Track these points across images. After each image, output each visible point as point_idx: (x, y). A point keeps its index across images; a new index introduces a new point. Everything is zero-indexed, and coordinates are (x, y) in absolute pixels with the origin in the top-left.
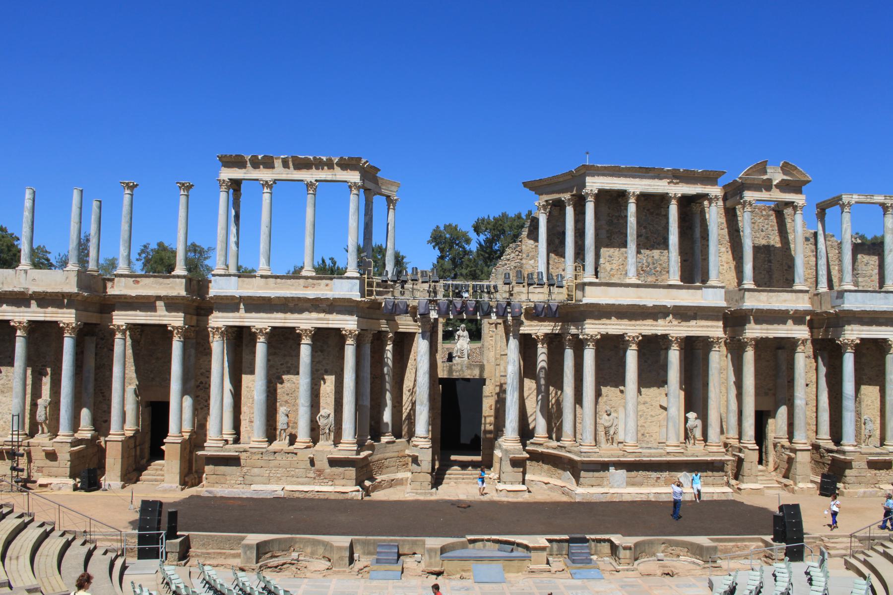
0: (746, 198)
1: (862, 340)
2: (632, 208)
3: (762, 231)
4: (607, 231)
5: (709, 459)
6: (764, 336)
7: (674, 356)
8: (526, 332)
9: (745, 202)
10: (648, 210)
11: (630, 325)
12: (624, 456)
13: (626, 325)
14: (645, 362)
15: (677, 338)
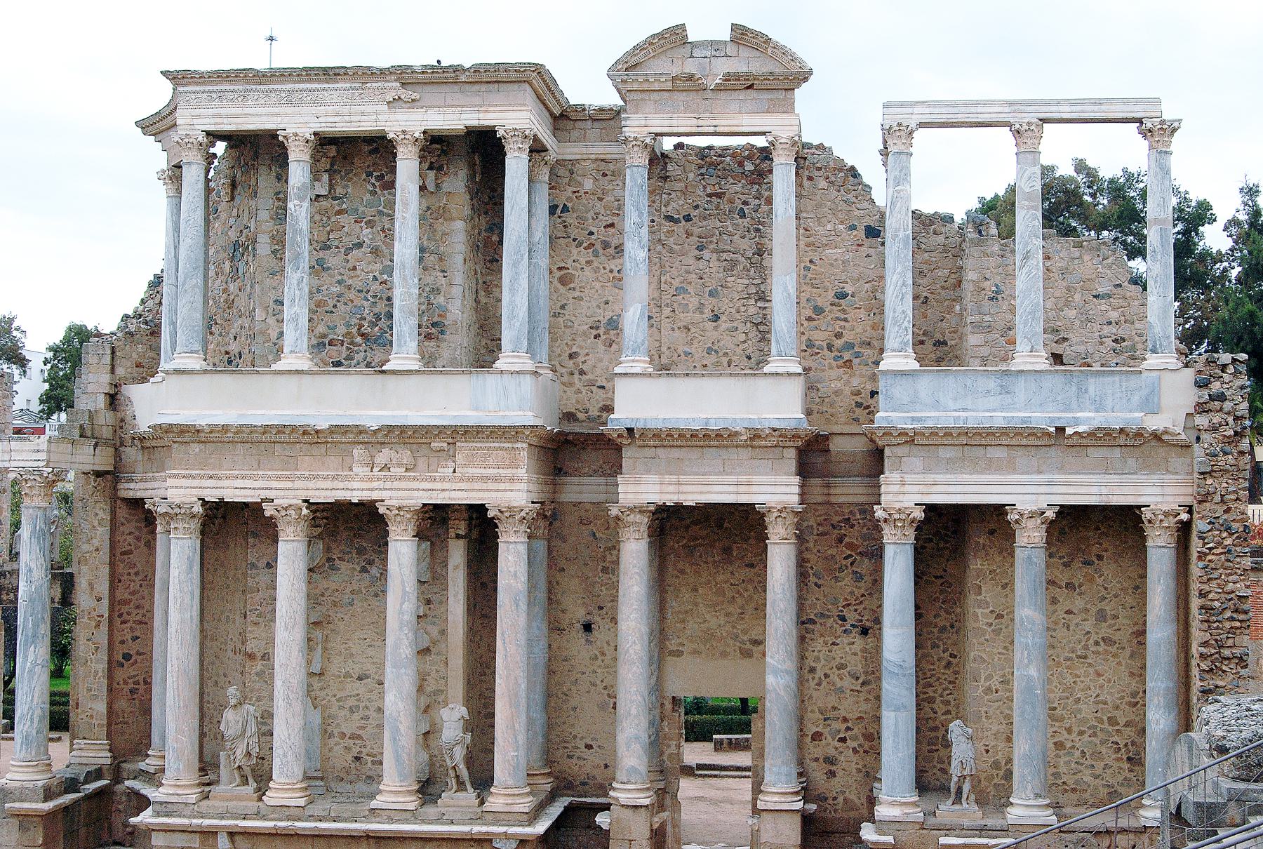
0: (628, 132)
1: (931, 509)
2: (298, 173)
3: (742, 215)
4: (273, 238)
5: (477, 829)
6: (670, 500)
7: (403, 551)
8: (139, 495)
9: (626, 140)
10: (378, 178)
11: (279, 478)
12: (258, 815)
13: (269, 478)
14: (364, 570)
15: (399, 508)
